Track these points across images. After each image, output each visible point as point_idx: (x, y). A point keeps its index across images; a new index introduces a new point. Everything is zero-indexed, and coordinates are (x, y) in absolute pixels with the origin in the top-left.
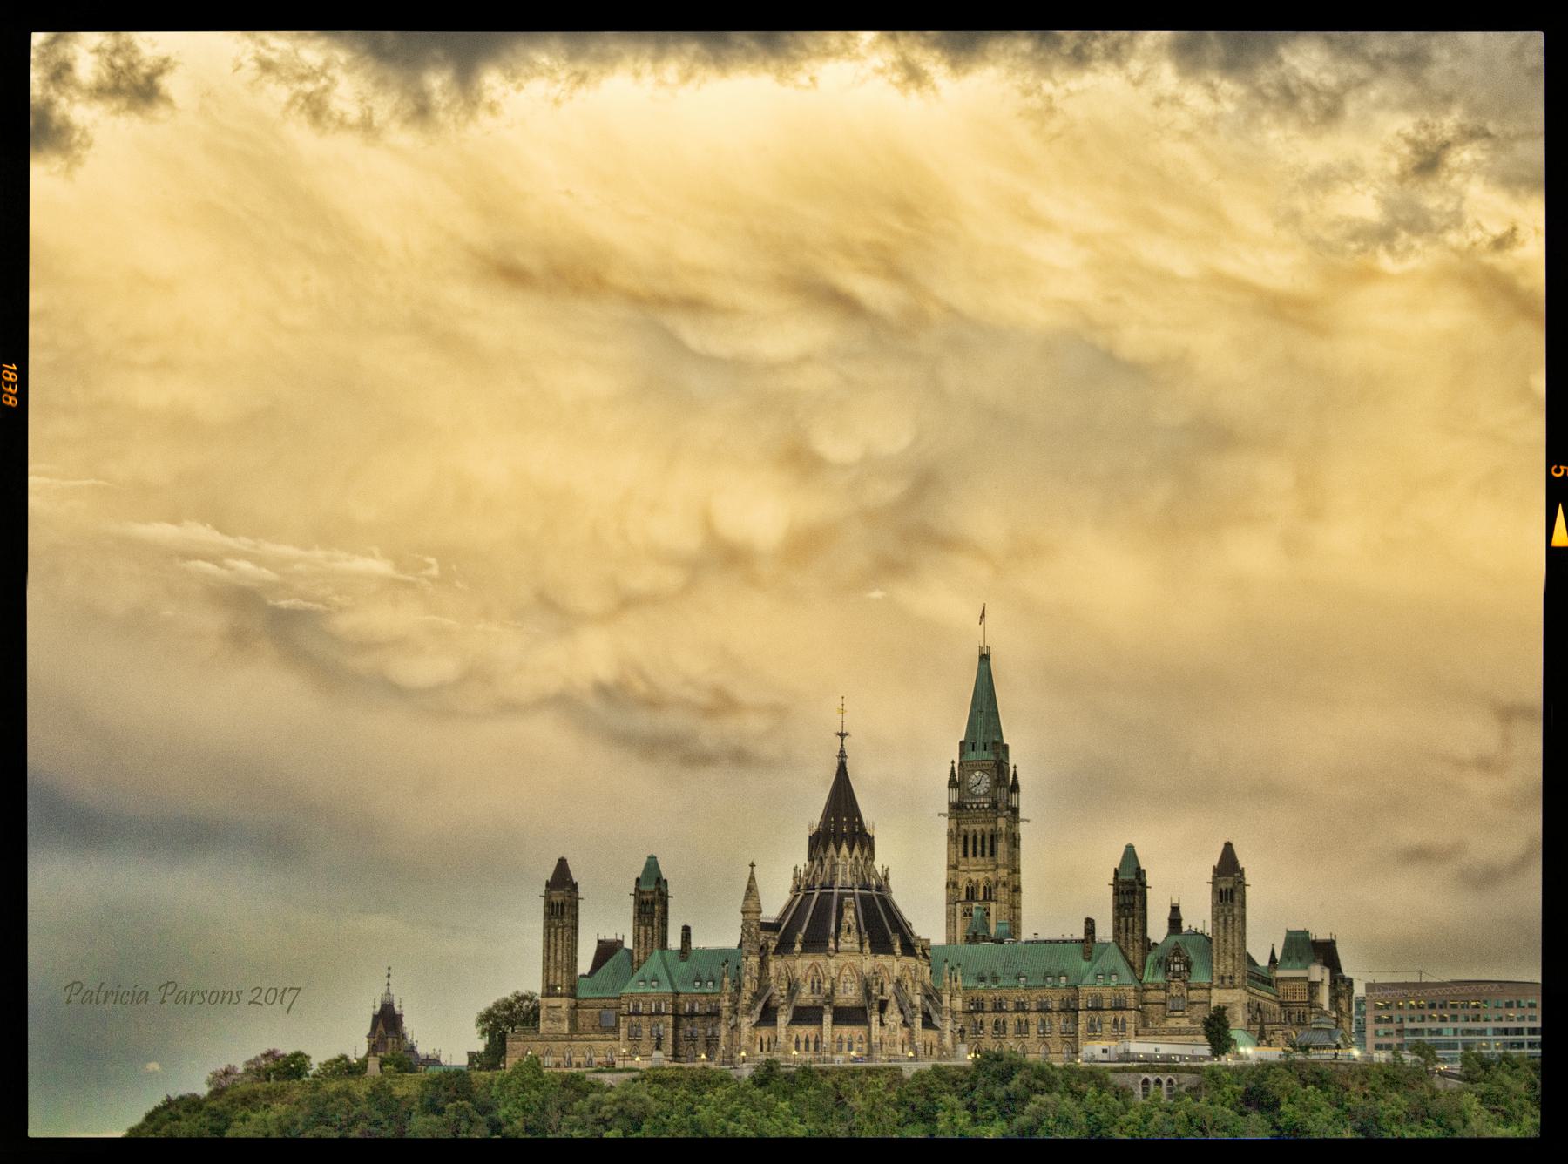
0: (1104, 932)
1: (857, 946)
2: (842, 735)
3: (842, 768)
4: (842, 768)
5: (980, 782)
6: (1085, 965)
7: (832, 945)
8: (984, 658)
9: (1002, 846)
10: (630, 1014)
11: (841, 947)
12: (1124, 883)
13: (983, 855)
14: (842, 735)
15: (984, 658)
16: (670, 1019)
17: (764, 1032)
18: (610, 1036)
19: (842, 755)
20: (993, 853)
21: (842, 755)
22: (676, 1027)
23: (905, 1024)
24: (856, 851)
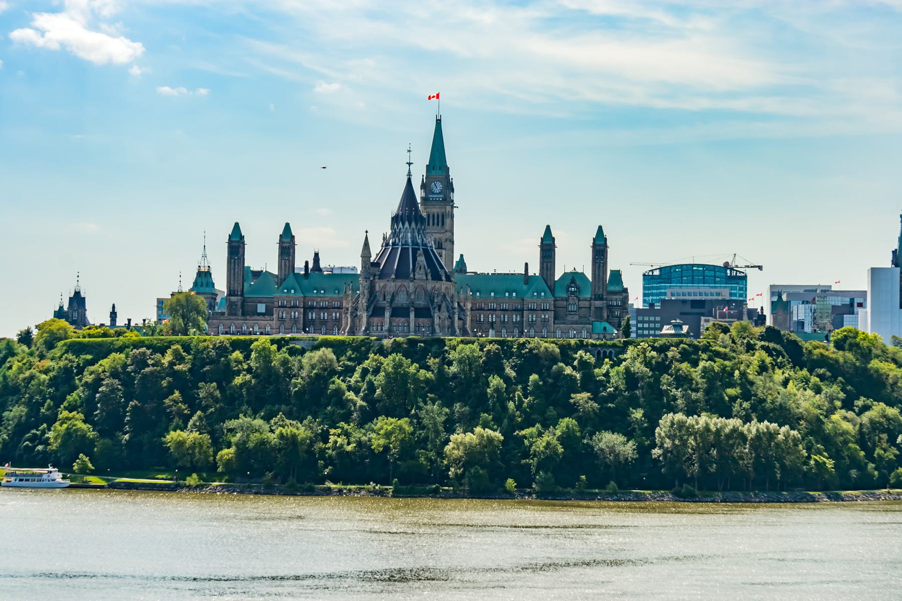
0: (535, 270)
1: (425, 278)
2: (410, 164)
3: (409, 181)
4: (409, 181)
5: (438, 187)
6: (525, 287)
7: (412, 276)
8: (439, 122)
9: (448, 221)
10: (279, 307)
11: (417, 276)
12: (546, 245)
13: (438, 225)
14: (410, 164)
15: (439, 122)
16: (302, 310)
17: (376, 320)
18: (267, 317)
19: (409, 174)
20: (443, 224)
21: (409, 174)
22: (305, 314)
23: (449, 317)
24: (413, 225)
